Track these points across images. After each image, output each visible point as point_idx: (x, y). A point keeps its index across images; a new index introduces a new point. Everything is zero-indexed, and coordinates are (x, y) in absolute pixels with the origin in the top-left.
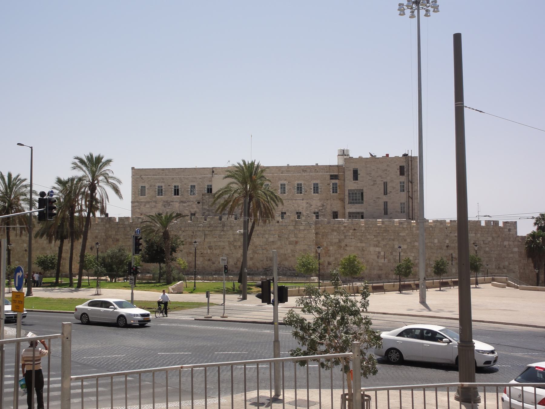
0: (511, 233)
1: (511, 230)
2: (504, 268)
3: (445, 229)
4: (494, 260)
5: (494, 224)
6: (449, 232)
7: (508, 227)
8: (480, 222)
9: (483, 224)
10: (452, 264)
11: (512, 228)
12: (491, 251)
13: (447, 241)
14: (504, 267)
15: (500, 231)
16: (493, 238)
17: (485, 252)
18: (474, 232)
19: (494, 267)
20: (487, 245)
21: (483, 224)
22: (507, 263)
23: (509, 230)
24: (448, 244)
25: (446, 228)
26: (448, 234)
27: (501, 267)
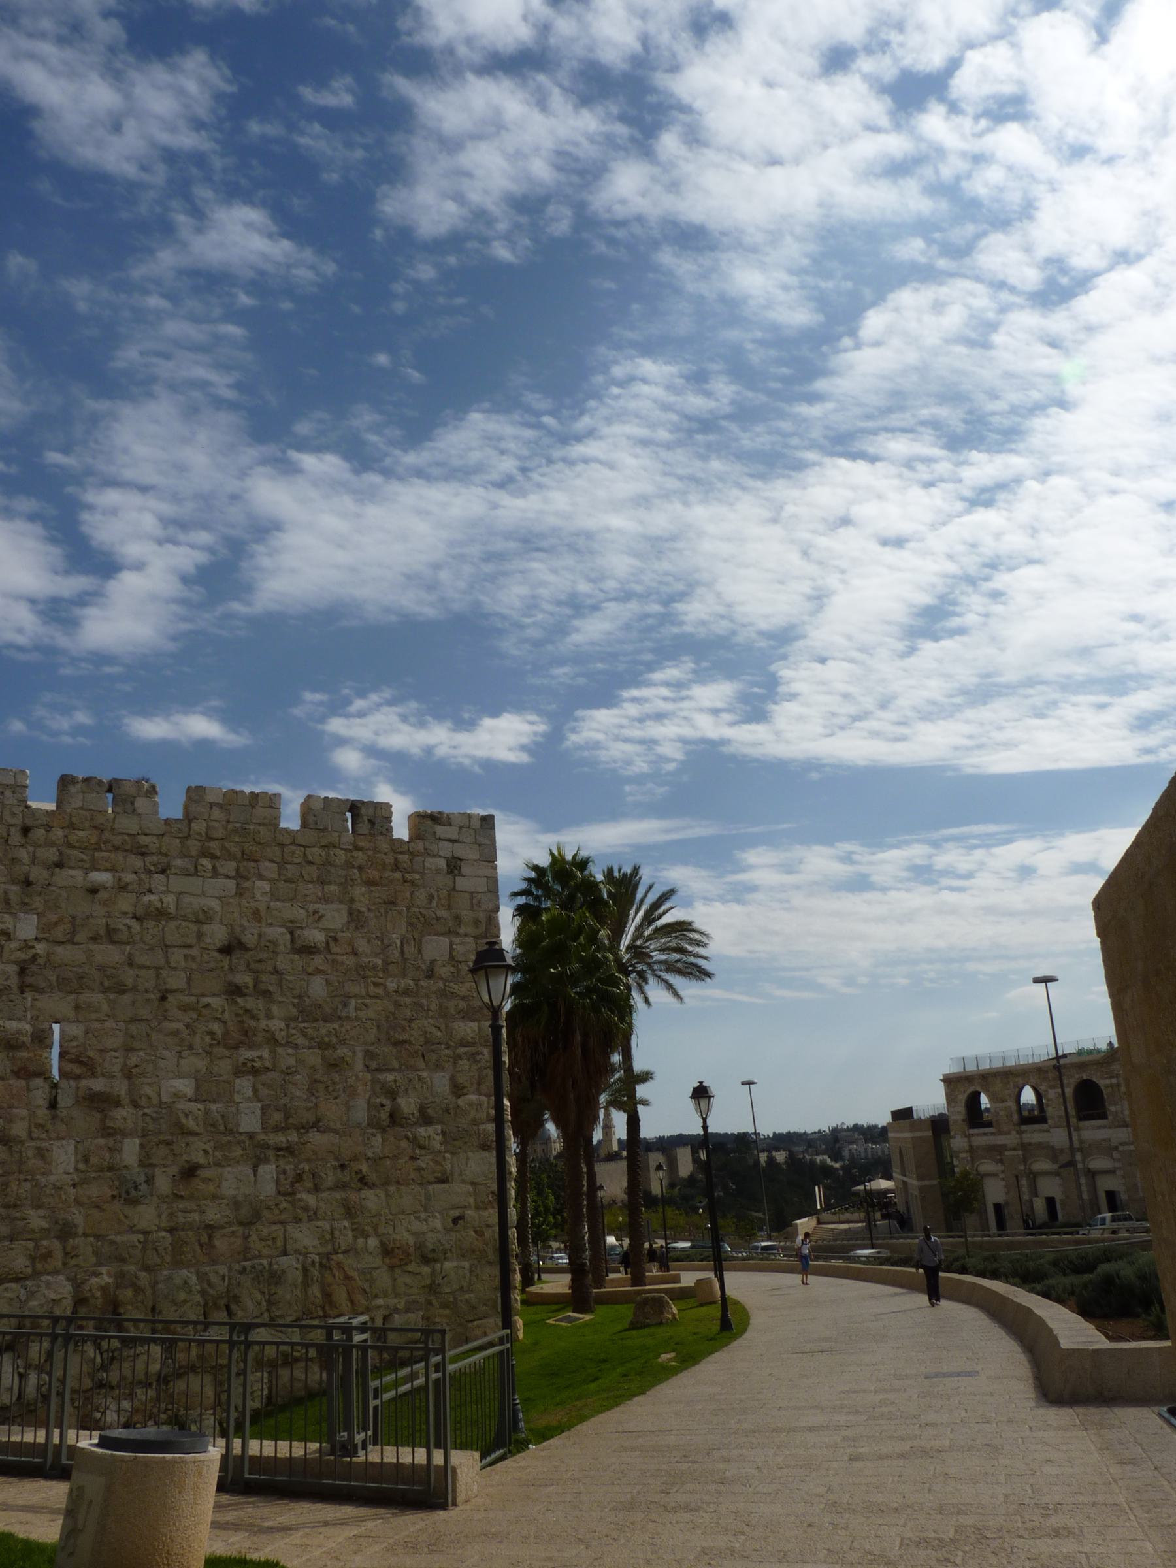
0: (461, 883)
1: (466, 869)
2: (427, 1120)
3: (16, 837)
4: (359, 1065)
5: (364, 828)
6: (51, 854)
7: (446, 849)
8: (273, 802)
9: (290, 820)
10: (53, 1105)
11: (465, 852)
12: (345, 1005)
13: (27, 927)
14: (422, 1110)
15: (396, 867)
16: (355, 919)
17: (307, 1012)
18: (229, 867)
19: (360, 1113)
20: (318, 961)
21: (290, 820)
22: (441, 1082)
23: (454, 866)
24: (26, 945)
25: (26, 831)
26: (37, 874)
27: (408, 1105)
